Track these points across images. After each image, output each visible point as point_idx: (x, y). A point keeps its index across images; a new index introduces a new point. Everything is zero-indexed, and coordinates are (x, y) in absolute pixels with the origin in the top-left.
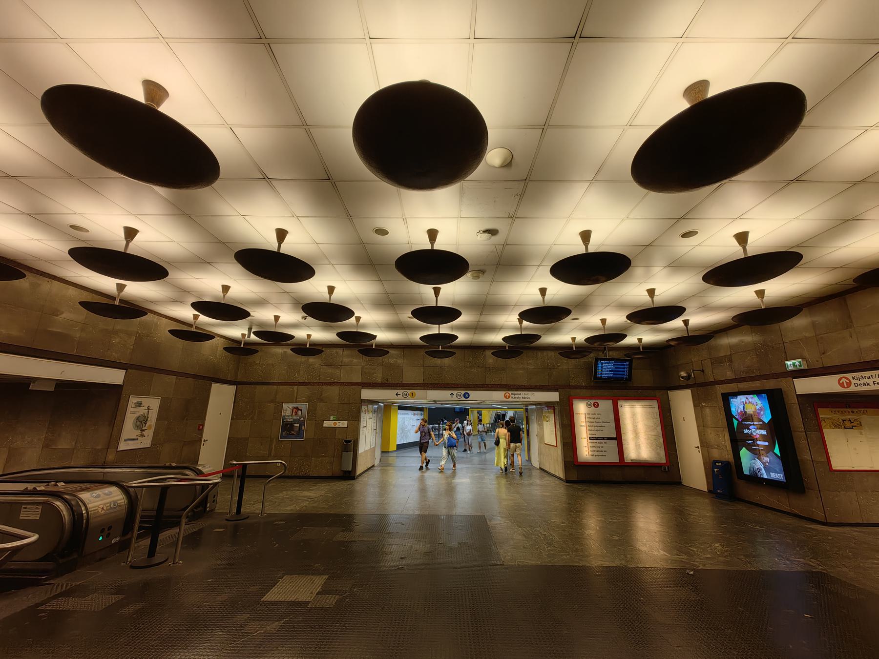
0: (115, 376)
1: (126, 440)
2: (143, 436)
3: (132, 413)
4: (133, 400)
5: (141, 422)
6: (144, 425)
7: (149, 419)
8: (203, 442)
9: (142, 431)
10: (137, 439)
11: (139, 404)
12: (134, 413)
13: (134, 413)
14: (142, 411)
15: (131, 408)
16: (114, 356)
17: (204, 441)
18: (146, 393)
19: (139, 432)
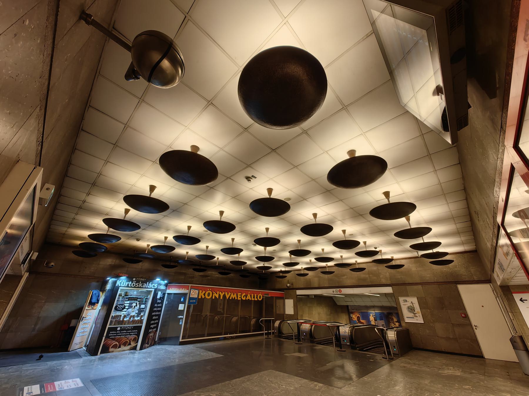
0: (389, 290)
1: (407, 317)
2: (416, 317)
3: (403, 305)
4: (401, 299)
5: (411, 309)
6: (414, 311)
7: (415, 308)
8: (474, 327)
9: (414, 314)
10: (414, 318)
11: (406, 301)
12: (405, 305)
13: (405, 305)
14: (409, 304)
15: (402, 303)
16: (384, 281)
17: (475, 326)
18: (407, 296)
19: (413, 315)
